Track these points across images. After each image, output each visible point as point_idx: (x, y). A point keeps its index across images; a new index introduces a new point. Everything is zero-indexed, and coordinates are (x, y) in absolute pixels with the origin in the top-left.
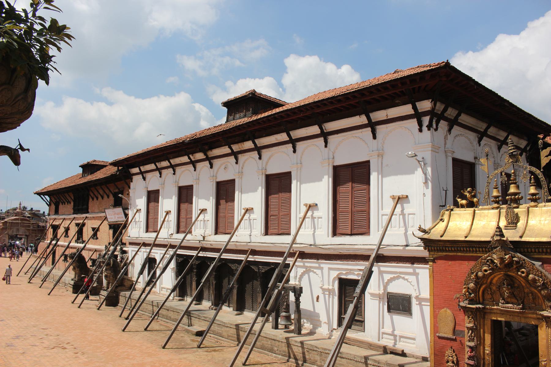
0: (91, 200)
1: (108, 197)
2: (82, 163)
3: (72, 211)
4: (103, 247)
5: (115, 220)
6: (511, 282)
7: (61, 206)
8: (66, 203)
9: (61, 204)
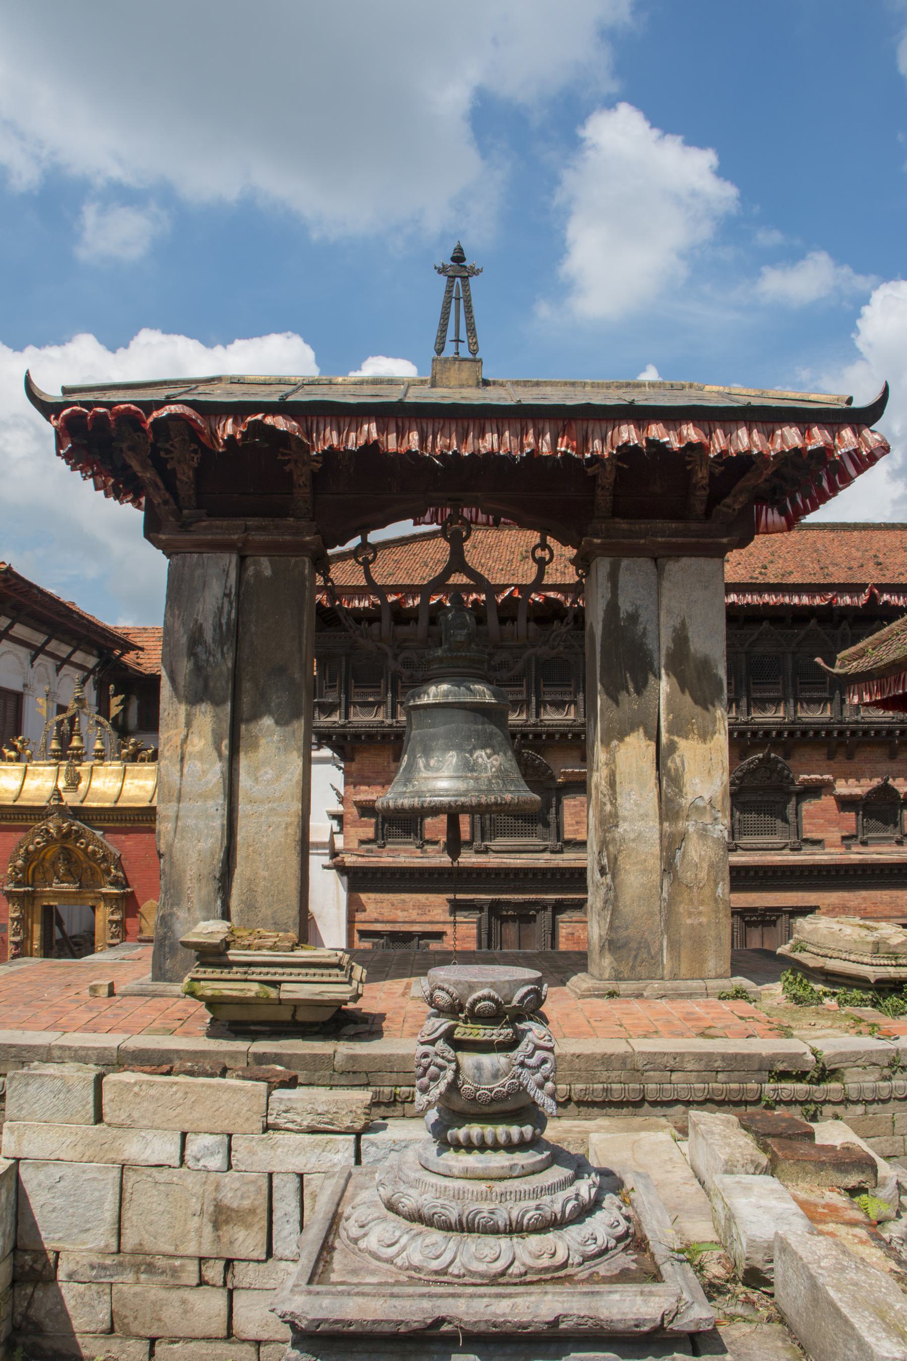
6: (68, 856)
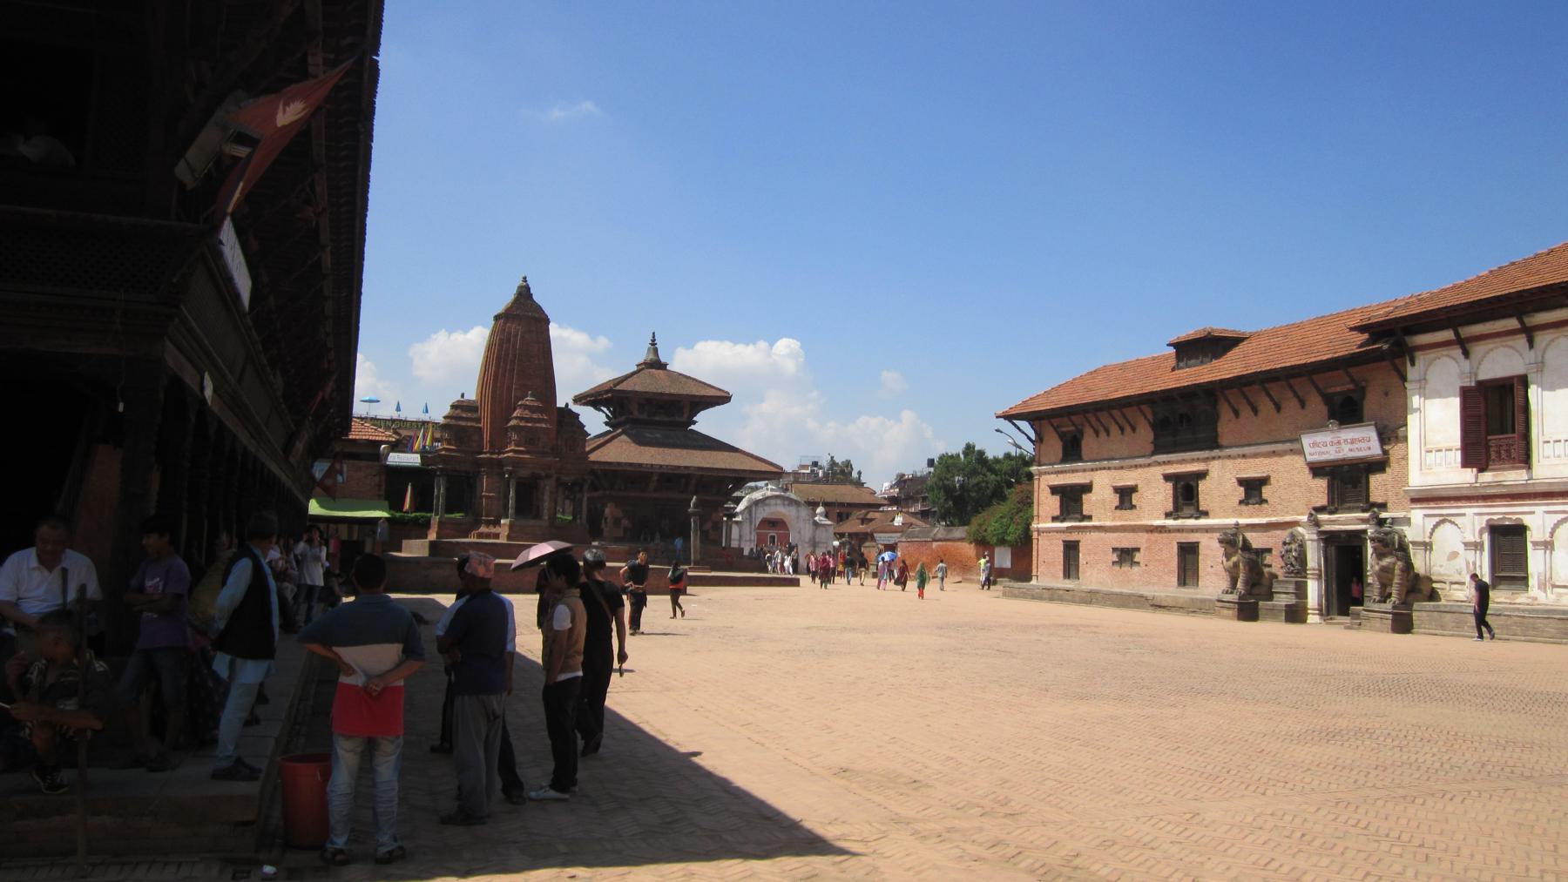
0: (1225, 414)
1: (1303, 404)
2: (1173, 338)
3: (1151, 447)
4: (1305, 518)
5: (1340, 456)
7: (1089, 443)
8: (1114, 429)
9: (1088, 432)
